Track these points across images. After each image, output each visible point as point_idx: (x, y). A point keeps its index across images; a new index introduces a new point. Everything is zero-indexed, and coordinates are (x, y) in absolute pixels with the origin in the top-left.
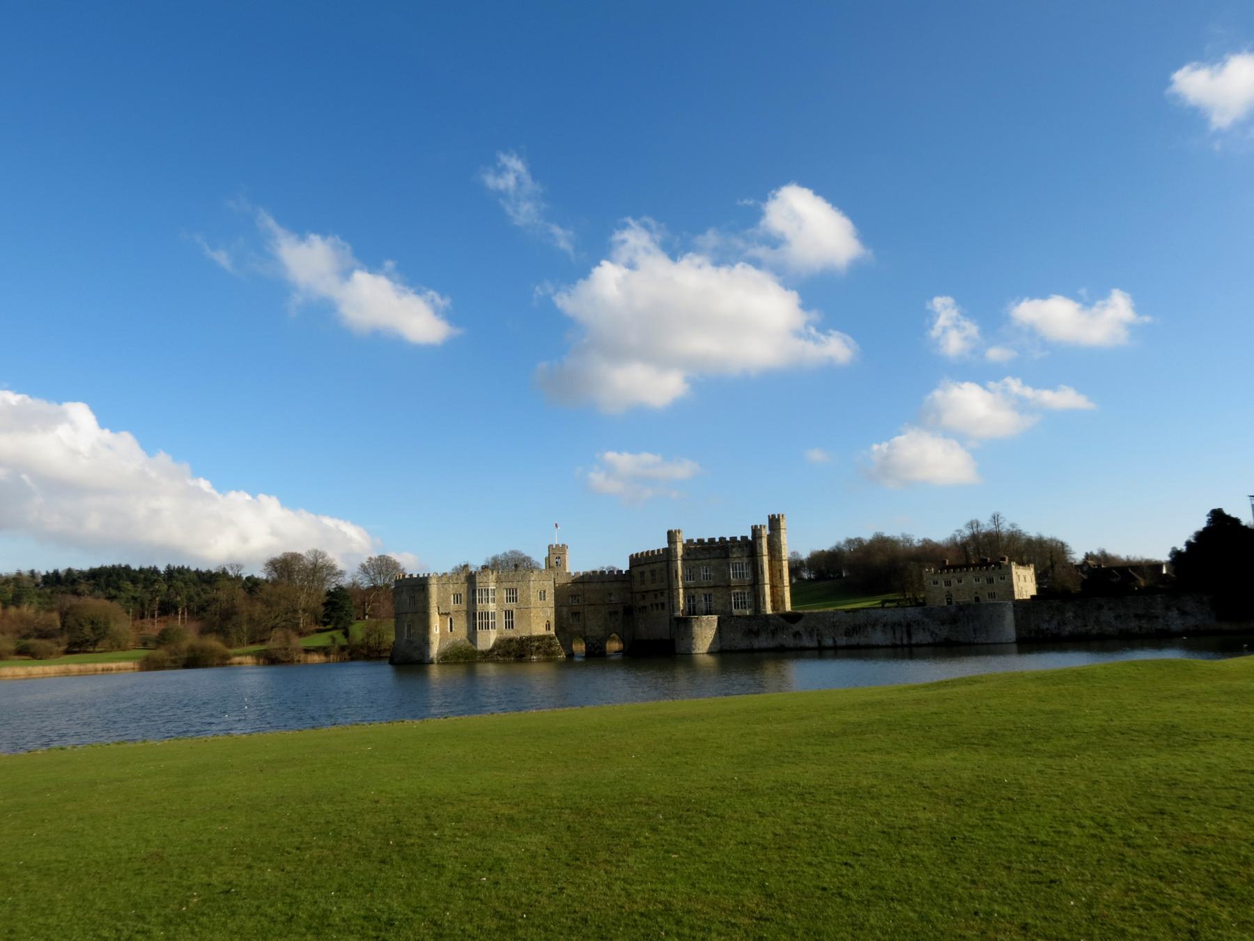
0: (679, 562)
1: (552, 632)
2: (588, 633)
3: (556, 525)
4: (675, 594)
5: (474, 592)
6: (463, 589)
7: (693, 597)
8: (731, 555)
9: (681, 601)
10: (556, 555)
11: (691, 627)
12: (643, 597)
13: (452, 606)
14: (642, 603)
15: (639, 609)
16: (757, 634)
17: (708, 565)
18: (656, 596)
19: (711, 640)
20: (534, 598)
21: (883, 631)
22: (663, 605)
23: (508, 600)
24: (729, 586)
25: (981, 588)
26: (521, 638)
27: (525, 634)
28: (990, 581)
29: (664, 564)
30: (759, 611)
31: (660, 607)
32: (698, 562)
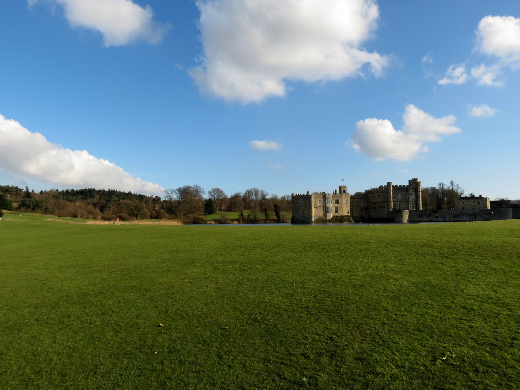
0: (392, 193)
1: (349, 214)
2: (354, 216)
3: (343, 180)
4: (390, 203)
5: (325, 200)
6: (322, 199)
7: (395, 204)
8: (409, 191)
9: (392, 205)
10: (342, 190)
11: (402, 214)
12: (374, 204)
13: (319, 205)
14: (374, 206)
15: (372, 208)
16: (422, 216)
17: (401, 194)
18: (381, 204)
19: (407, 218)
20: (344, 203)
21: (467, 217)
22: (384, 207)
23: (336, 203)
24: (408, 201)
25: (475, 205)
26: (340, 216)
27: (341, 215)
28: (479, 203)
29: (386, 193)
30: (418, 210)
31: (383, 207)
32: (398, 193)
